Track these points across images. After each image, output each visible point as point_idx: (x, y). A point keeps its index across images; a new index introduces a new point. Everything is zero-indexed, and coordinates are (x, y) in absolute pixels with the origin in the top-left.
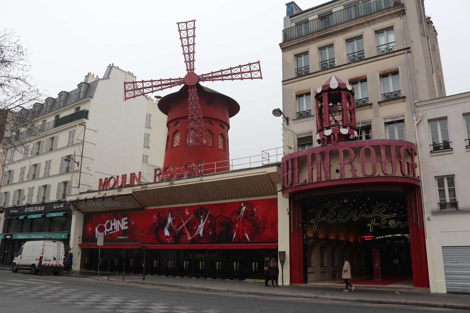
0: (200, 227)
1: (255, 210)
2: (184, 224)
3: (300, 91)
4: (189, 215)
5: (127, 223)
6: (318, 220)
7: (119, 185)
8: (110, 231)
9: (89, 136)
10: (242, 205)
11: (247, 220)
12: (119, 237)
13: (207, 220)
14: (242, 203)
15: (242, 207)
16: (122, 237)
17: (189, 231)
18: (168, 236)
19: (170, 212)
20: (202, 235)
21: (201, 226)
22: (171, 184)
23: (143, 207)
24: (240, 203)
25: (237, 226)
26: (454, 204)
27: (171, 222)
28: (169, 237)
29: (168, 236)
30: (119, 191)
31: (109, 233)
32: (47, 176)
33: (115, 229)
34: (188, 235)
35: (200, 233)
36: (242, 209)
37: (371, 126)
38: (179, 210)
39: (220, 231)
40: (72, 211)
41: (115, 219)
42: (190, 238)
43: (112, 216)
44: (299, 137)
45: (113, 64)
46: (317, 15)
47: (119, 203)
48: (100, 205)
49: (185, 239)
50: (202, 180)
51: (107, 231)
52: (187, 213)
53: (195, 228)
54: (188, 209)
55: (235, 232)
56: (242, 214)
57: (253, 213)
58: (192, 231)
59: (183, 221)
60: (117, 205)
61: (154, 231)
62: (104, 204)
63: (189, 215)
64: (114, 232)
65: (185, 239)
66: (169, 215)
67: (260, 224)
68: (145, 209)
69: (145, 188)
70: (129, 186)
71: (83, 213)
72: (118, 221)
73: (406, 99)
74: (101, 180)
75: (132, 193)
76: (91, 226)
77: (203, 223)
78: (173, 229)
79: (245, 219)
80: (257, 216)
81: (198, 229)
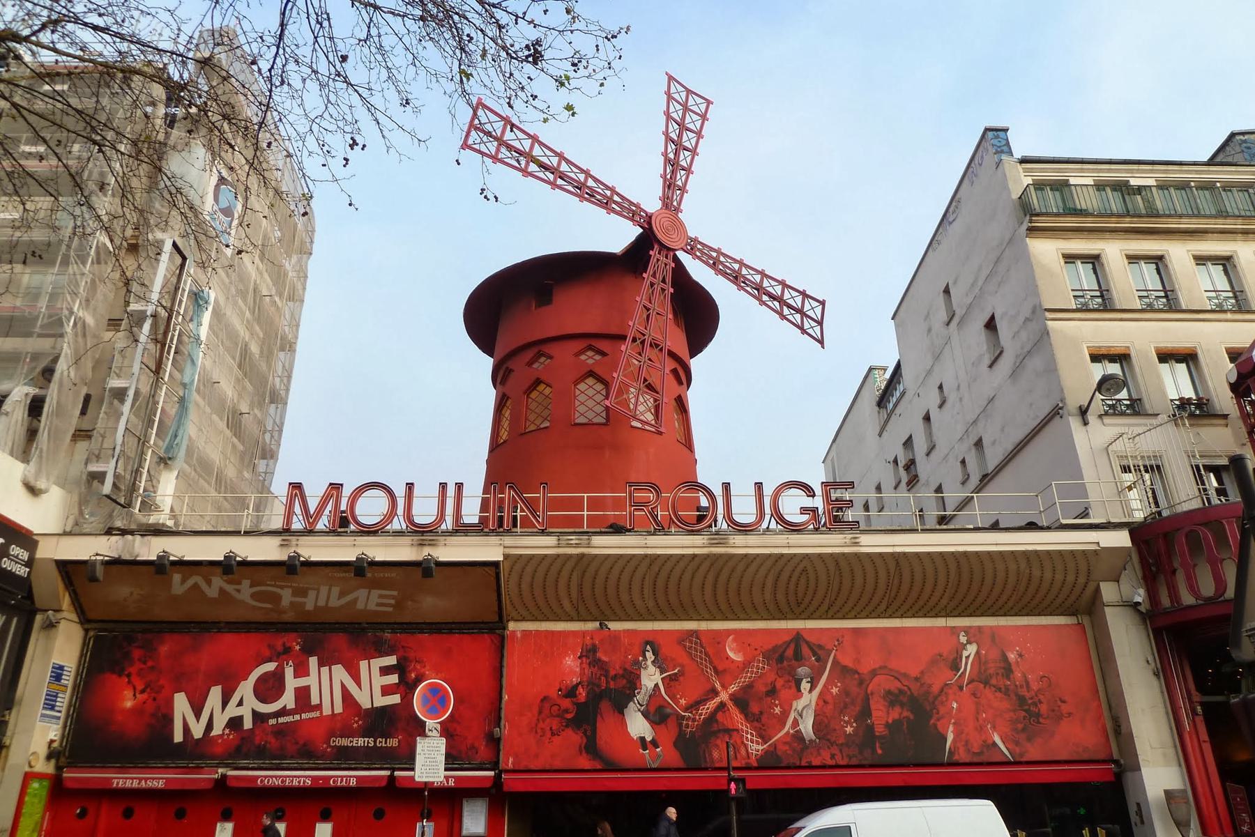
0: (800, 708)
1: (1013, 656)
2: (724, 696)
3: (1100, 347)
4: (746, 664)
5: (393, 679)
8: (283, 712)
10: (963, 639)
12: (345, 742)
14: (963, 633)
15: (964, 647)
16: (360, 742)
18: (649, 739)
20: (814, 738)
22: (711, 545)
24: (955, 631)
25: (955, 705)
27: (656, 685)
28: (654, 743)
29: (649, 739)
31: (272, 722)
33: (315, 700)
35: (803, 731)
36: (965, 654)
38: (696, 644)
39: (890, 721)
41: (313, 661)
42: (760, 748)
43: (298, 648)
47: (381, 596)
50: (856, 544)
51: (254, 713)
53: (777, 710)
54: (735, 640)
55: (951, 728)
56: (967, 667)
57: (1008, 669)
60: (369, 601)
61: (569, 716)
66: (644, 656)
67: (1041, 702)
69: (577, 546)
72: (340, 672)
75: (501, 559)
76: (140, 687)
77: (810, 691)
78: (668, 710)
79: (982, 686)
80: (1025, 676)
81: (792, 716)
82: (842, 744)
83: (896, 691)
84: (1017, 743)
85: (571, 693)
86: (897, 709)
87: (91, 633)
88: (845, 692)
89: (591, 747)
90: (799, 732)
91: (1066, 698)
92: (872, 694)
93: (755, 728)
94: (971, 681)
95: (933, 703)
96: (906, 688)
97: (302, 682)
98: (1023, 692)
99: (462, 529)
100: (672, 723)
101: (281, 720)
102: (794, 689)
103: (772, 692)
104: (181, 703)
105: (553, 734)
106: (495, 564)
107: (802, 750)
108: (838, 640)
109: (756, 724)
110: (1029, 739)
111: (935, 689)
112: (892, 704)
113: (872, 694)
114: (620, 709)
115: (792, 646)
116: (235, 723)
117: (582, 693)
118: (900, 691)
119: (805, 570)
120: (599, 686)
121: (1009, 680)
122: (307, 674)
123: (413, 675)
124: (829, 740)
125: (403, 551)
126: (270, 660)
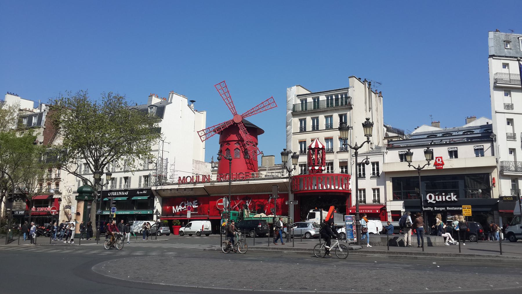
2: (236, 205)
5: (197, 204)
7: (194, 181)
8: (185, 209)
9: (166, 147)
10: (270, 196)
23: (209, 194)
24: (269, 194)
30: (194, 185)
37: (333, 162)
40: (155, 195)
41: (188, 201)
44: (300, 164)
46: (311, 98)
48: (178, 192)
50: (249, 183)
60: (191, 193)
62: (181, 192)
68: (210, 196)
70: (201, 183)
71: (161, 197)
72: (190, 202)
73: (349, 152)
74: (180, 177)
80: (278, 202)
97: (186, 204)
99: (200, 183)
101: (185, 210)
104: (173, 207)
106: (203, 187)
111: (265, 204)
112: (258, 206)
116: (180, 210)
119: (243, 186)
122: (187, 203)
125: (191, 186)
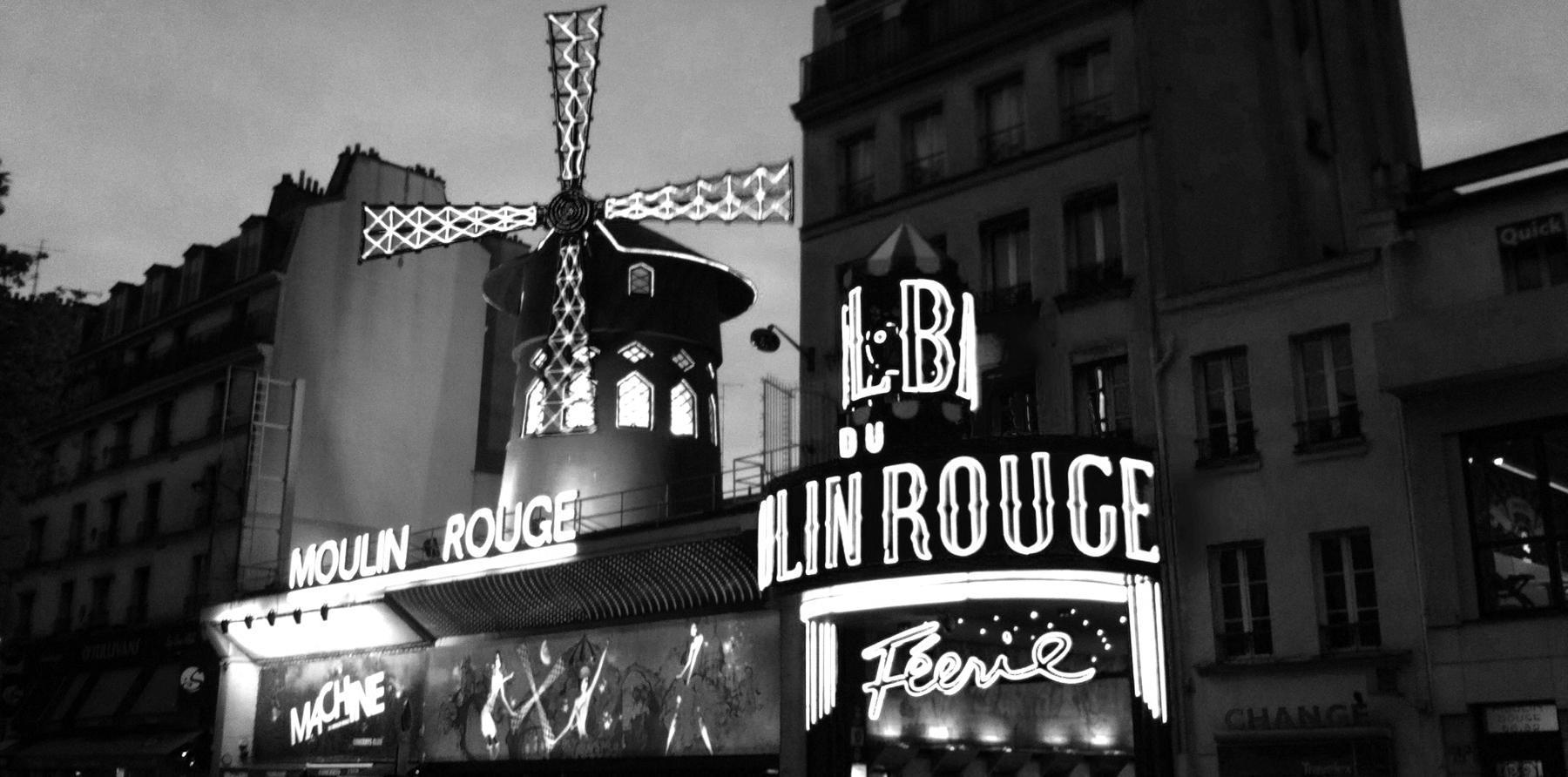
2: (536, 698)
5: (381, 692)
6: (884, 684)
8: (334, 721)
11: (704, 681)
13: (600, 682)
15: (692, 639)
17: (551, 716)
18: (492, 737)
19: (498, 656)
21: (583, 702)
26: (1263, 638)
28: (495, 740)
29: (492, 737)
32: (151, 534)
33: (346, 714)
34: (547, 731)
39: (634, 717)
45: (358, 147)
49: (539, 745)
52: (546, 660)
53: (566, 708)
54: (549, 646)
55: (674, 722)
57: (722, 662)
58: (558, 719)
59: (533, 687)
61: (454, 718)
63: (551, 667)
64: (345, 723)
65: (539, 745)
66: (494, 663)
67: (741, 694)
71: (255, 661)
78: (504, 711)
81: (574, 712)
82: (600, 740)
83: (640, 688)
84: (718, 737)
85: (456, 696)
86: (640, 704)
87: (260, 668)
88: (608, 689)
89: (462, 744)
90: (576, 728)
91: (762, 691)
92: (625, 690)
93: (551, 725)
94: (694, 674)
95: (664, 697)
96: (647, 684)
98: (730, 685)
100: (505, 723)
102: (577, 689)
103: (563, 693)
105: (445, 733)
106: (379, 601)
107: (577, 744)
108: (609, 639)
109: (552, 721)
110: (727, 732)
111: (667, 685)
112: (637, 700)
113: (625, 690)
114: (479, 710)
115: (580, 647)
116: (315, 729)
117: (461, 698)
118: (645, 687)
120: (469, 691)
121: (721, 670)
123: (390, 688)
124: (593, 735)
126: (329, 680)
